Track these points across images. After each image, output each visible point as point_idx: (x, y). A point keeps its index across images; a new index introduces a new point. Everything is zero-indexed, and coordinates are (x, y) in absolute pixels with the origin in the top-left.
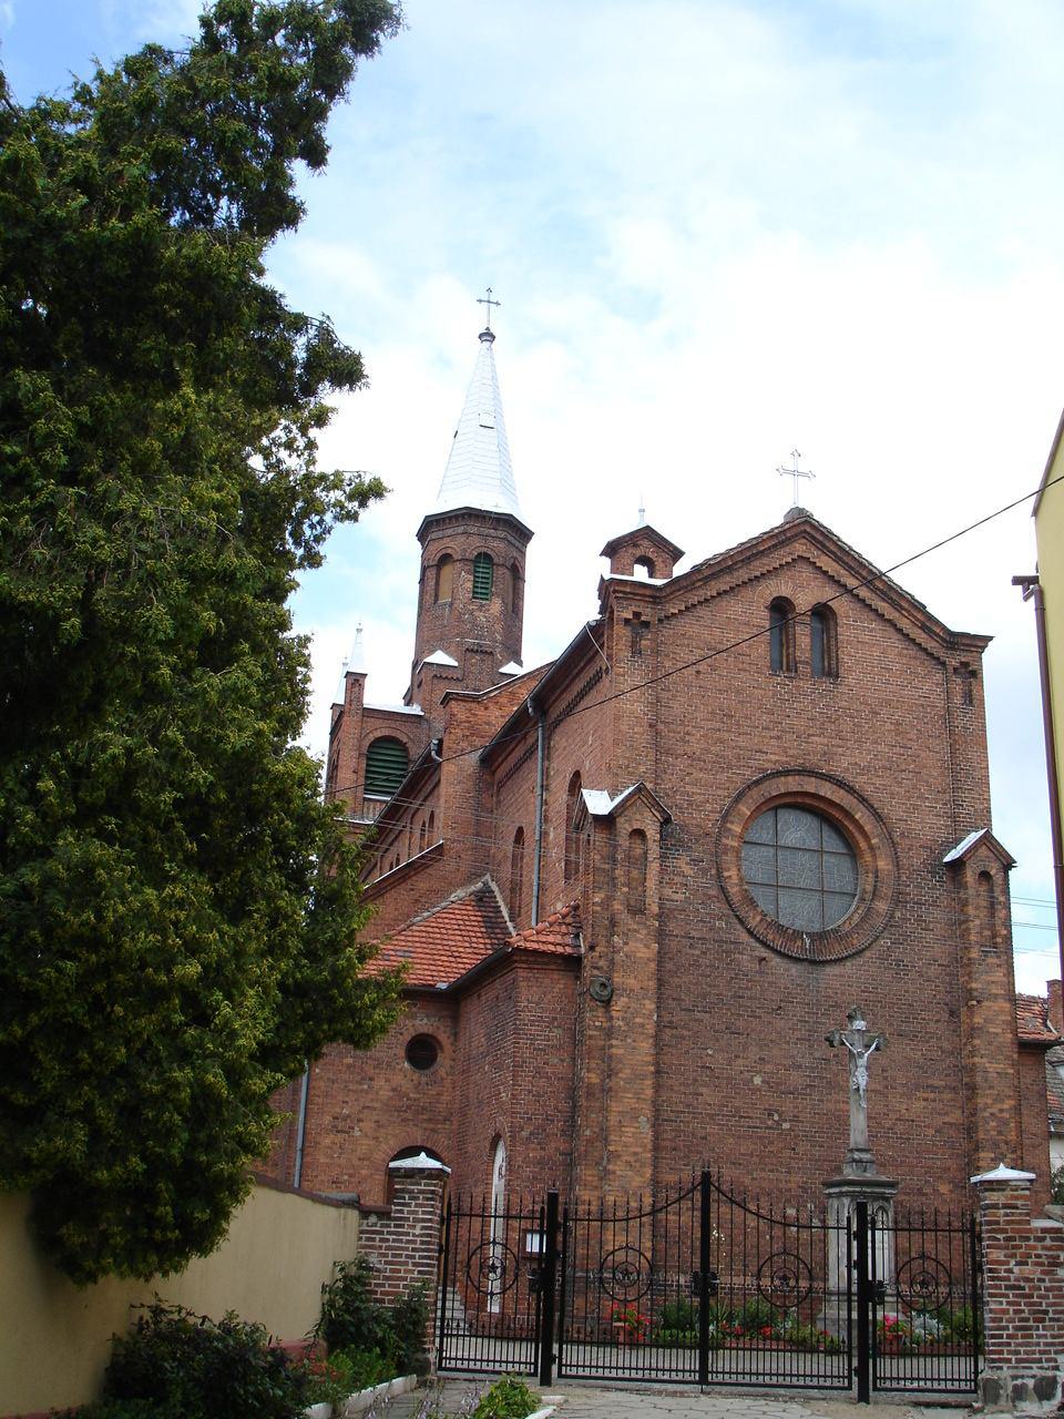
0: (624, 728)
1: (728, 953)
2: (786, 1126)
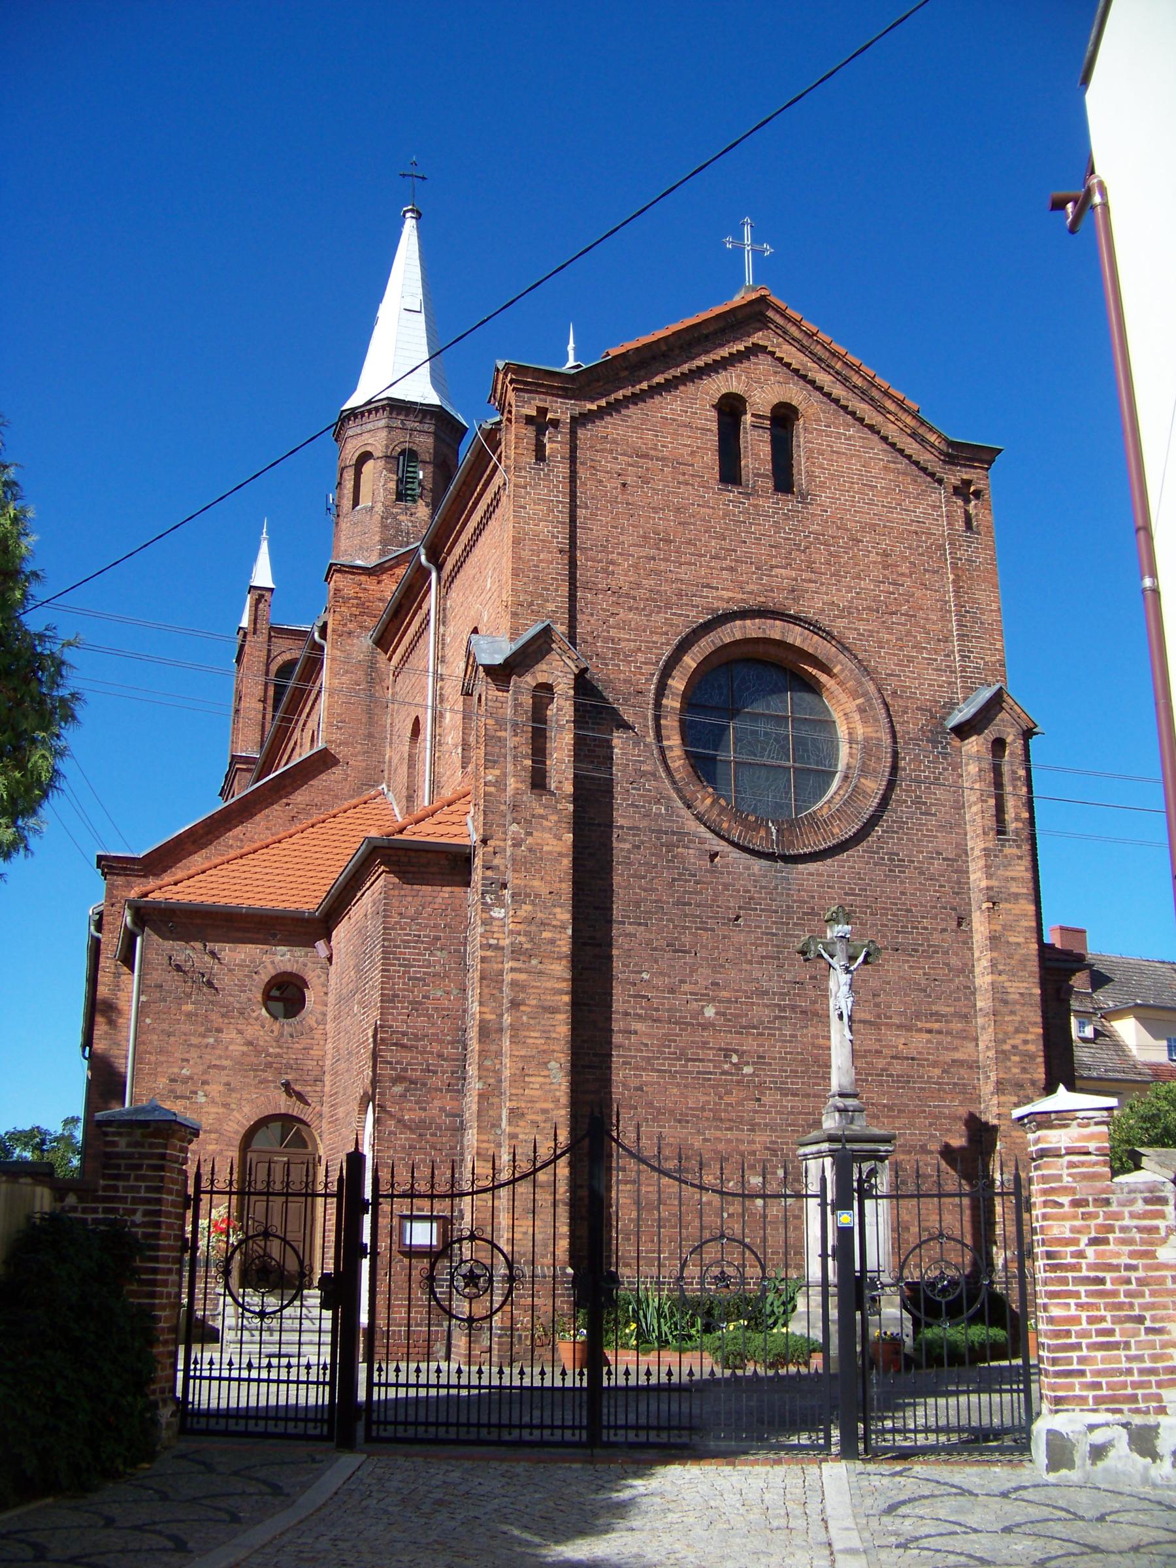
0: (525, 554)
1: (670, 846)
2: (748, 1070)
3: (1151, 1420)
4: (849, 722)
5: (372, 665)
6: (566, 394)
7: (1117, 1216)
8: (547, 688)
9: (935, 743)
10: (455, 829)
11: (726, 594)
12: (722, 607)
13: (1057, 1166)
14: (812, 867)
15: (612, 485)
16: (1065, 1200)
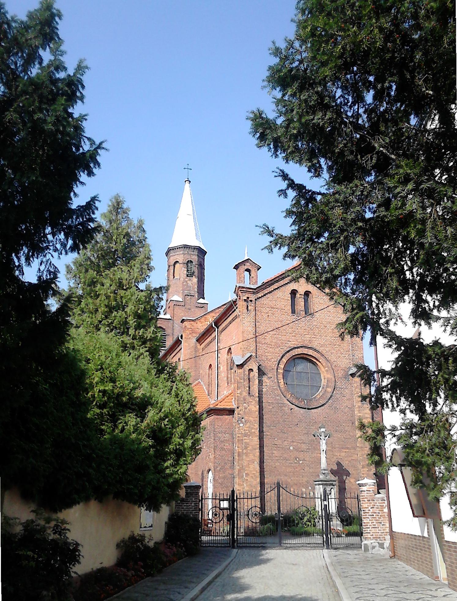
0: (245, 335)
1: (281, 407)
2: (301, 462)
3: (383, 542)
4: (325, 375)
5: (196, 347)
6: (254, 293)
7: (376, 503)
8: (251, 370)
9: (346, 378)
10: (230, 404)
11: (293, 343)
12: (292, 346)
13: (364, 494)
14: (315, 410)
15: (265, 316)
16: (366, 500)
